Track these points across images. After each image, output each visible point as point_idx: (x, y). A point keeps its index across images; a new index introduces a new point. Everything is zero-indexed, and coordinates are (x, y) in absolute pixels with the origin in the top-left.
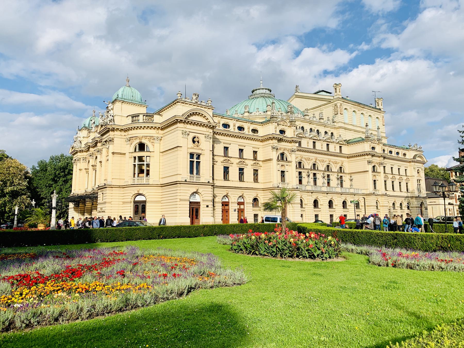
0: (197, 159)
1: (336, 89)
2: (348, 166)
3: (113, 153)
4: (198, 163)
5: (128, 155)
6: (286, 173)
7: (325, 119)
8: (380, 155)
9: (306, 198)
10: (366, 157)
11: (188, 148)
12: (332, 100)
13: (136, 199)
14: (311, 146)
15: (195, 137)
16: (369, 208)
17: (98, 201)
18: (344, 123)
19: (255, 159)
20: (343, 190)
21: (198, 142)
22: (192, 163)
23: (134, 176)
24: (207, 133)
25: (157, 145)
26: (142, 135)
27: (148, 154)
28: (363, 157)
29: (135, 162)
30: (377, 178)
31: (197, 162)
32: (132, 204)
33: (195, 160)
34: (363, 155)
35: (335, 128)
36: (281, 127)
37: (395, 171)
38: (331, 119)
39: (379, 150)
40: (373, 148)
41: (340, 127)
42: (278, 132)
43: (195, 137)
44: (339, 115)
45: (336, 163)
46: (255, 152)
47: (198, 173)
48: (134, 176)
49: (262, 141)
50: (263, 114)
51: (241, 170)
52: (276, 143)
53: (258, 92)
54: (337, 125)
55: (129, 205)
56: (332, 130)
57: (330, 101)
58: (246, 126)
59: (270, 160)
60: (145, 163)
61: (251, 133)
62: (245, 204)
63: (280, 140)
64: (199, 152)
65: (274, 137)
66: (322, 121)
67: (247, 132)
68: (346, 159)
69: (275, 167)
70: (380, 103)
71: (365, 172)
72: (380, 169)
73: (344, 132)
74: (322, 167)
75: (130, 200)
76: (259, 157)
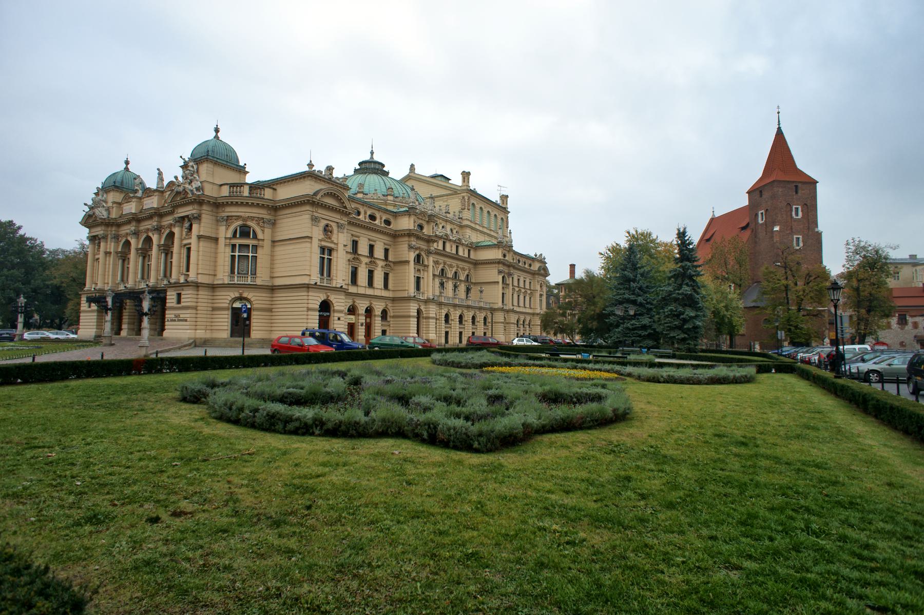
3: (200, 237)
4: (330, 260)
5: (222, 241)
7: (452, 213)
13: (234, 306)
14: (441, 247)
15: (327, 226)
17: (168, 305)
20: (470, 303)
23: (232, 272)
24: (342, 222)
26: (247, 215)
27: (255, 242)
29: (233, 250)
32: (230, 312)
33: (326, 257)
36: (421, 221)
38: (457, 214)
40: (505, 256)
41: (467, 226)
45: (463, 269)
46: (386, 251)
47: (329, 275)
50: (382, 197)
51: (371, 273)
53: (367, 165)
55: (226, 312)
58: (378, 215)
60: (250, 255)
61: (383, 225)
62: (373, 318)
63: (418, 238)
64: (332, 246)
69: (411, 271)
72: (509, 281)
75: (226, 305)
76: (390, 258)
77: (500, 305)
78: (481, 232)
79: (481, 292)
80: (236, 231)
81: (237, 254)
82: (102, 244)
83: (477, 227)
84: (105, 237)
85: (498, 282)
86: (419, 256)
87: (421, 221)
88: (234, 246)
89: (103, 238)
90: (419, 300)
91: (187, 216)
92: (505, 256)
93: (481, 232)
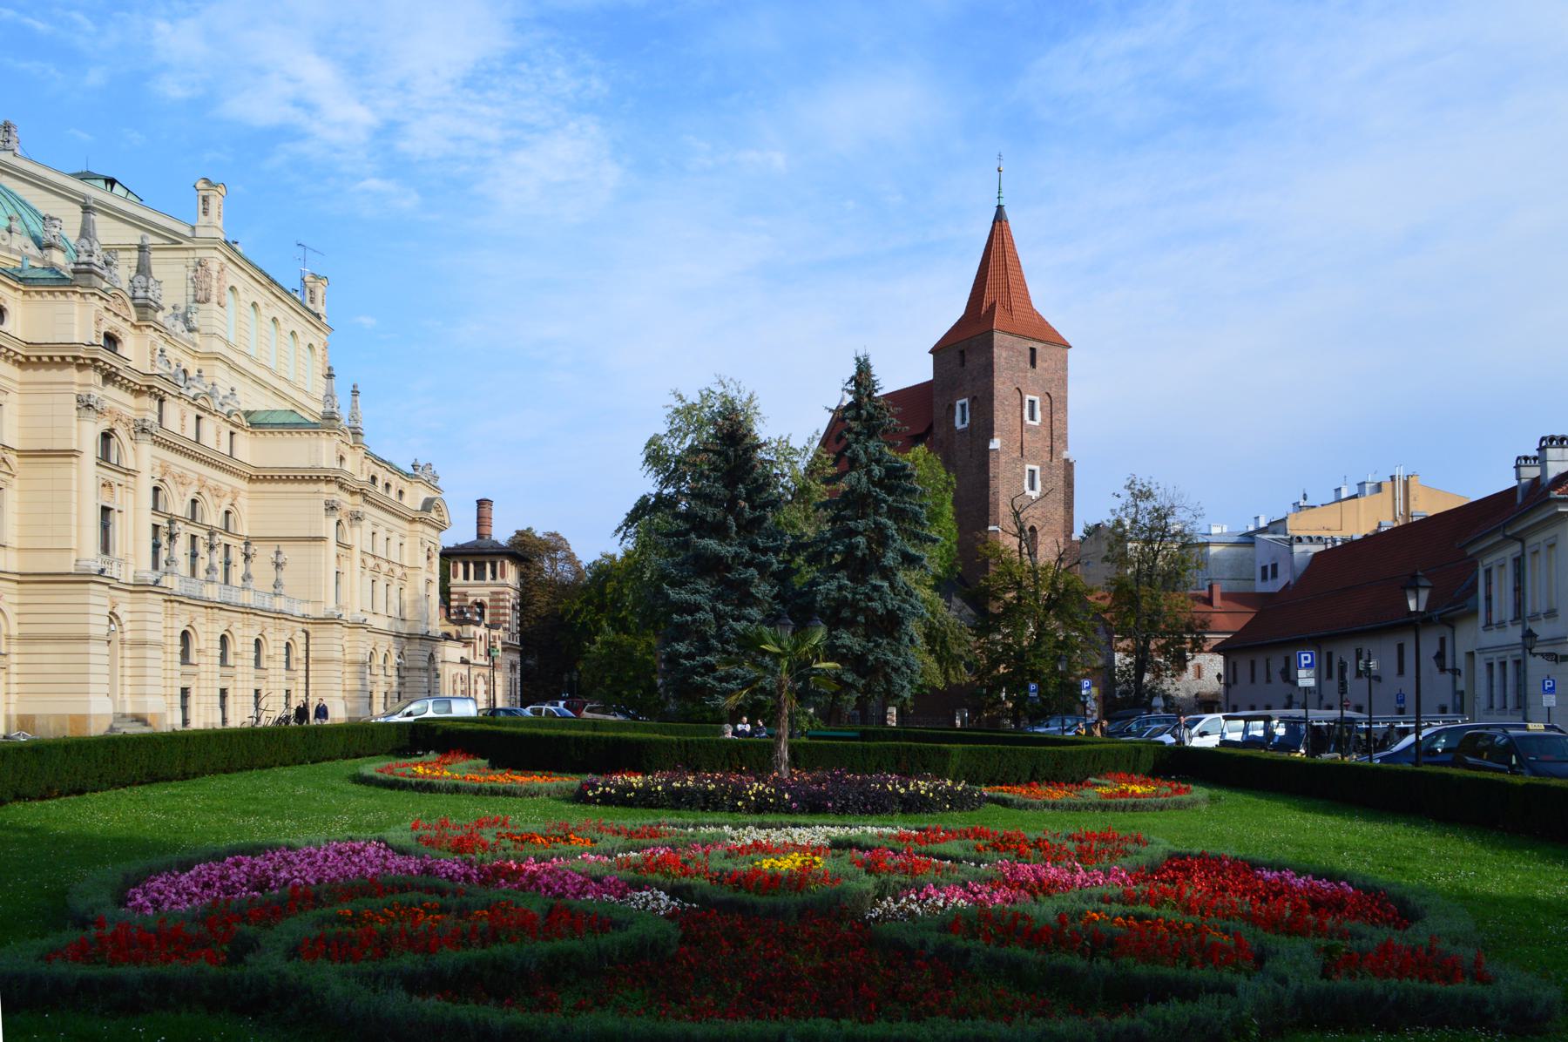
1: (205, 200)
6: (115, 518)
8: (356, 487)
9: (204, 628)
10: (323, 487)
16: (320, 666)
18: (227, 343)
28: (312, 487)
30: (345, 566)
35: (196, 355)
41: (216, 357)
49: (25, 363)
54: (204, 345)
59: (70, 454)
65: (95, 360)
68: (242, 485)
70: (319, 292)
71: (315, 539)
77: (329, 607)
78: (257, 381)
79: (278, 565)
83: (241, 361)
85: (322, 539)
86: (106, 436)
87: (118, 322)
90: (112, 584)
92: (342, 458)
93: (257, 381)
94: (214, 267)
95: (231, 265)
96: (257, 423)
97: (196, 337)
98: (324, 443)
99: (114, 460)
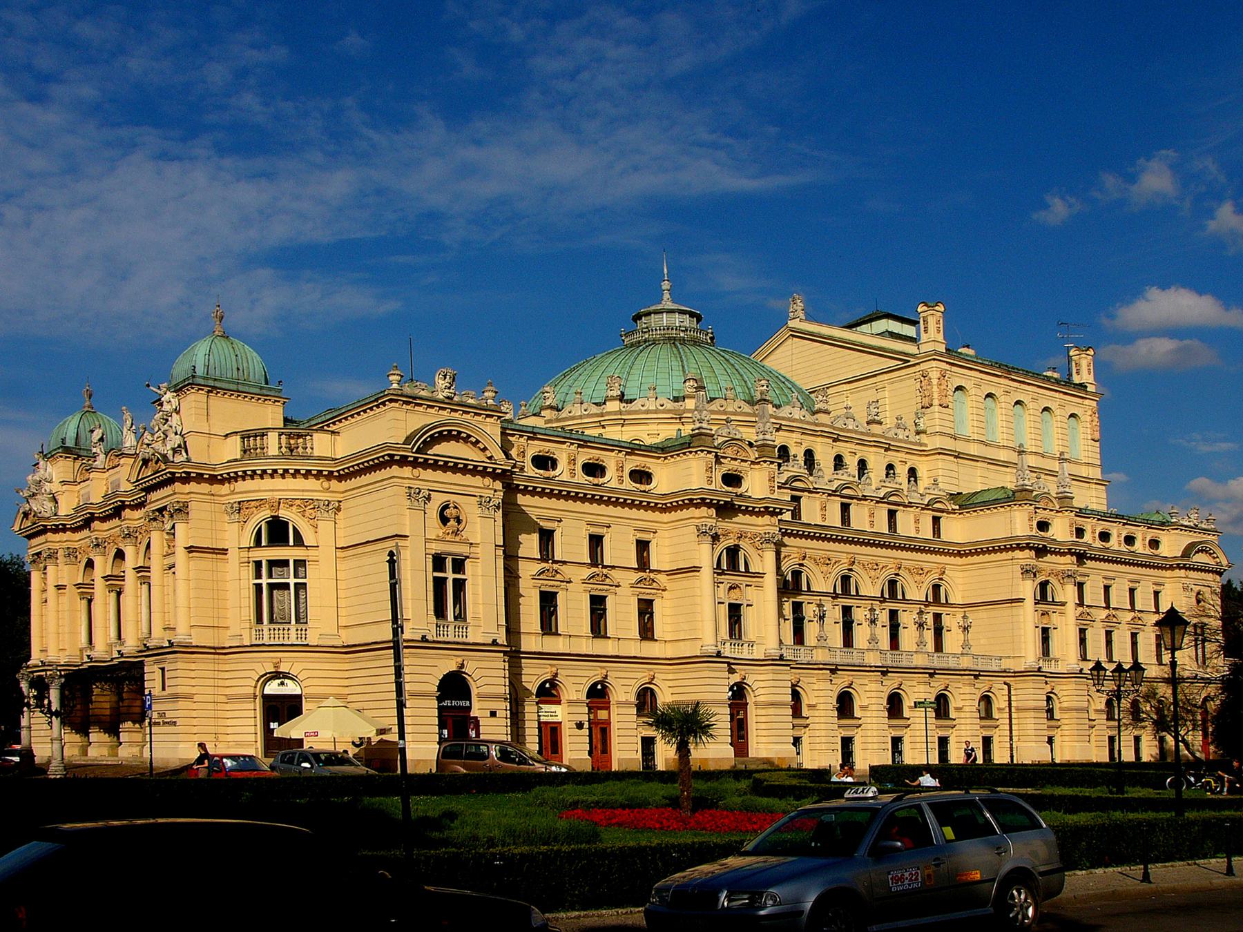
0: (454, 572)
2: (962, 582)
4: (460, 586)
5: (233, 555)
7: (889, 422)
8: (1065, 549)
10: (1018, 554)
11: (427, 540)
12: (913, 356)
14: (835, 519)
15: (446, 507)
19: (643, 563)
21: (459, 521)
22: (439, 584)
25: (325, 527)
29: (258, 576)
31: (454, 580)
34: (1006, 549)
37: (1119, 597)
39: (1061, 531)
40: (1043, 526)
42: (717, 484)
43: (446, 507)
44: (936, 408)
48: (259, 620)
49: (665, 509)
52: (711, 517)
56: (912, 461)
57: (905, 361)
60: (292, 581)
64: (463, 550)
66: (876, 429)
67: (615, 478)
73: (954, 467)
74: (870, 586)
78: (992, 462)
80: (260, 529)
81: (264, 581)
82: (50, 569)
84: (53, 555)
88: (258, 564)
89: (50, 556)
91: (165, 508)
93: (992, 462)
94: (934, 375)
95: (954, 369)
96: (966, 503)
97: (924, 438)
98: (1017, 513)
99: (742, 568)
